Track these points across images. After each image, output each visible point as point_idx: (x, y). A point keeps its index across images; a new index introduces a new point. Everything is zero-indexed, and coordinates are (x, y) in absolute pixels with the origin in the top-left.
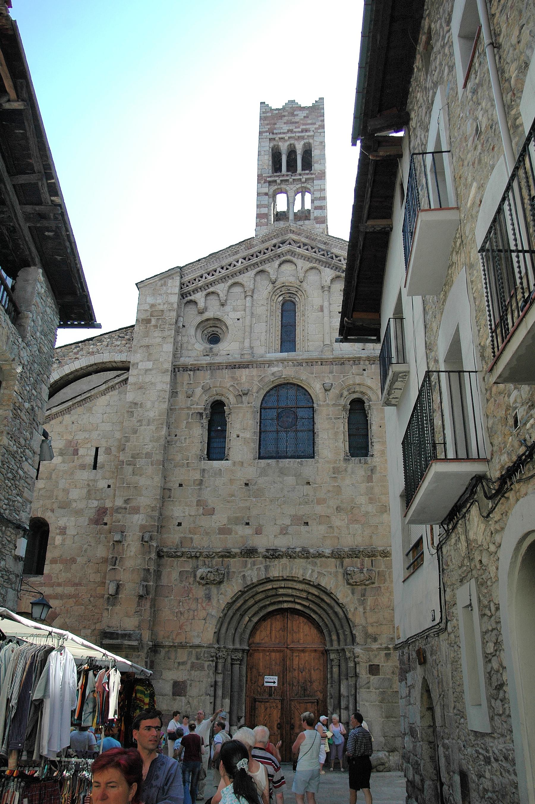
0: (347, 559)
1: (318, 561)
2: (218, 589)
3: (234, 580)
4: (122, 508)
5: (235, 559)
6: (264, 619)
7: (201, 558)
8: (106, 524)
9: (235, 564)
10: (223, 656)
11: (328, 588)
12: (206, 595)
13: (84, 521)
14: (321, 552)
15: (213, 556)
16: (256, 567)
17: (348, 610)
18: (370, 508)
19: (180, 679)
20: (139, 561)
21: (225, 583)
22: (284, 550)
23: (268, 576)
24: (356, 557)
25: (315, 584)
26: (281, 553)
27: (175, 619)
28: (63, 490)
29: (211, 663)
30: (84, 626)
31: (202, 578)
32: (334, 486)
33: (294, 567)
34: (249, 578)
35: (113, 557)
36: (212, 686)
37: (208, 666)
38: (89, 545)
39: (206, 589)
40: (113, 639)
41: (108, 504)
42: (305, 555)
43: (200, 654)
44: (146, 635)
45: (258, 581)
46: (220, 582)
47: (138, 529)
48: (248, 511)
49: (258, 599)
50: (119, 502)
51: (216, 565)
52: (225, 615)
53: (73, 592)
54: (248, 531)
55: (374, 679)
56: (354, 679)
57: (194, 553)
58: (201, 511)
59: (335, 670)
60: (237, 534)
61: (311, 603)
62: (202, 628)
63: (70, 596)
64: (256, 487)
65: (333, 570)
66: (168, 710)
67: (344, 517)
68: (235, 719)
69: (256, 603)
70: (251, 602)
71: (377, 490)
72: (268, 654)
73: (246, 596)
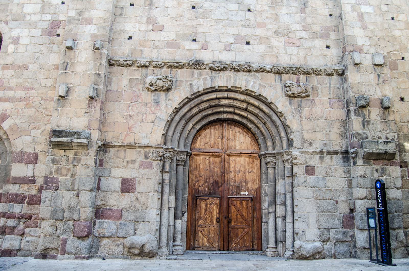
0: (285, 75)
1: (259, 74)
2: (166, 95)
3: (182, 88)
4: (75, 19)
5: (182, 70)
6: (204, 127)
7: (150, 68)
8: (59, 35)
9: (181, 74)
10: (171, 156)
11: (268, 98)
12: (154, 100)
13: (37, 32)
14: (262, 67)
15: (162, 65)
16: (203, 77)
17: (287, 118)
18: (304, 34)
19: (129, 177)
20: (91, 66)
21: (173, 91)
22: (228, 63)
23: (213, 86)
24: (292, 73)
25: (257, 94)
26: (226, 66)
27: (125, 121)
28: (18, 4)
29: (159, 162)
30: (34, 127)
31: (152, 85)
32: (272, 14)
33: (238, 79)
34: (196, 87)
35: (64, 62)
36: (159, 184)
37: (156, 165)
38: (41, 53)
39: (155, 96)
40: (63, 137)
41: (62, 18)
42: (248, 68)
43: (149, 153)
44: (95, 135)
45: (204, 90)
46: (168, 89)
47: (89, 38)
48: (195, 29)
49: (202, 107)
50: (72, 14)
51: (165, 74)
52: (172, 119)
53: (24, 96)
54: (195, 46)
55: (311, 179)
56: (291, 178)
57: (144, 62)
58: (151, 27)
59: (271, 171)
60: (184, 48)
61: (249, 114)
62: (151, 130)
63: (21, 100)
64: (202, 10)
65: (273, 83)
66: (117, 205)
67: (281, 39)
68: (179, 213)
69: (200, 111)
70: (195, 110)
71: (309, 20)
72: (207, 158)
73: (193, 103)
